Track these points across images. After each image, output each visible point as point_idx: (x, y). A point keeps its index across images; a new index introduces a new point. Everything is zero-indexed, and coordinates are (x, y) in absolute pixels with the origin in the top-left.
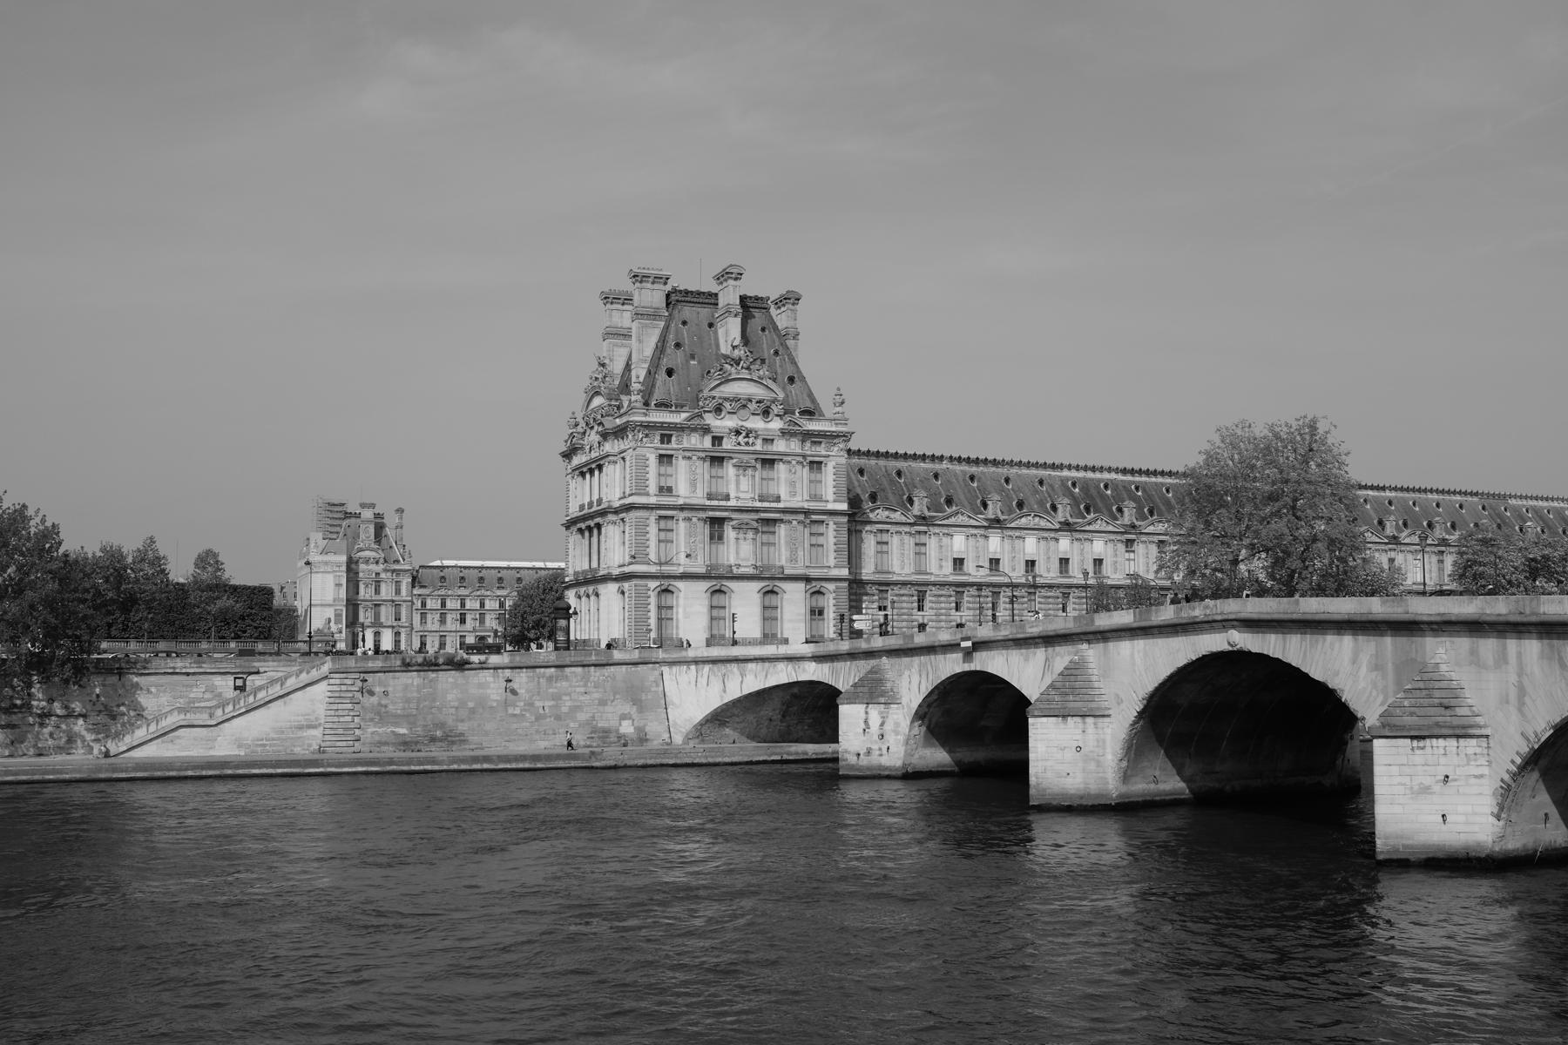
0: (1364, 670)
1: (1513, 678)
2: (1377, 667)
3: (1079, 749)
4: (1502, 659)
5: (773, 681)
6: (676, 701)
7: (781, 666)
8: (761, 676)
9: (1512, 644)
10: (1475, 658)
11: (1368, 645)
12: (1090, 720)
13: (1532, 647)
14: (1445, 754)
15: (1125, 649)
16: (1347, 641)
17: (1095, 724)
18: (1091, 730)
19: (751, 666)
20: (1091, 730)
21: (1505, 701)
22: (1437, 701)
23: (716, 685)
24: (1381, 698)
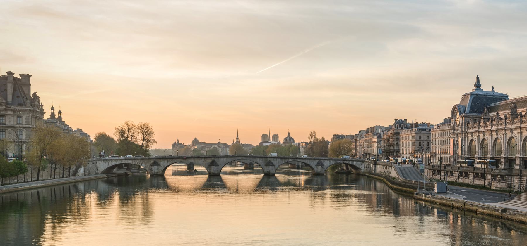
0: (261, 161)
1: (277, 161)
2: (263, 161)
4: (276, 160)
5: (117, 163)
6: (99, 166)
8: (115, 163)
9: (277, 159)
10: (274, 160)
11: (261, 159)
13: (279, 159)
15: (222, 159)
16: (259, 159)
21: (276, 163)
23: (107, 164)
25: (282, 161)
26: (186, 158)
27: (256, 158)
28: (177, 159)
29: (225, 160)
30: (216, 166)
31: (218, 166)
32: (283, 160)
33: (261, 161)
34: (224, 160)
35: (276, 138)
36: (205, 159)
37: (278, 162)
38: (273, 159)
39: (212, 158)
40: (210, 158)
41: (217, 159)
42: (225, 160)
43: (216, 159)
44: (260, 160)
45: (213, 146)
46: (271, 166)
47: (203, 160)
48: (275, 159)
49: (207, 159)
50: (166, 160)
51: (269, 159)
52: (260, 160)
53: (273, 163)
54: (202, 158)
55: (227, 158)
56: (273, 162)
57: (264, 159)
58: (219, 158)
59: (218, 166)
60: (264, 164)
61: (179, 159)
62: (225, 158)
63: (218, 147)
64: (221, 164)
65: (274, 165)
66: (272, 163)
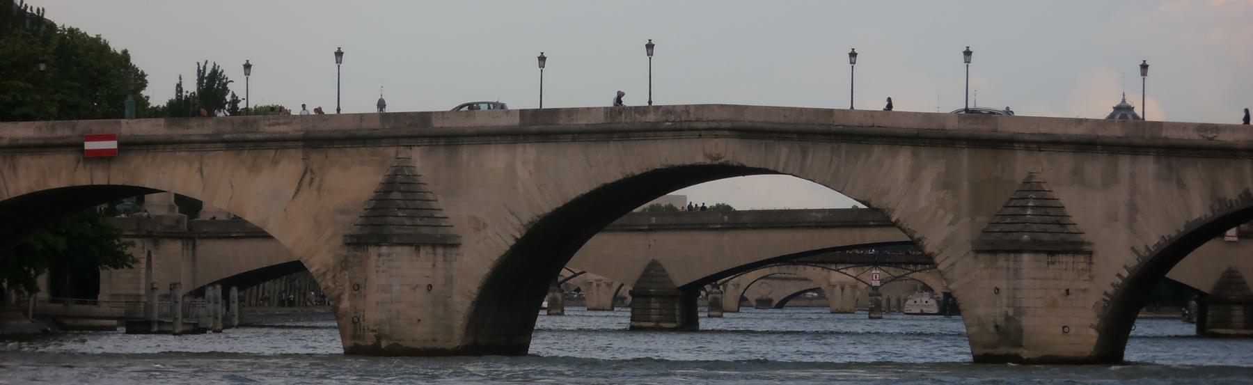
0: (927, 187)
2: (947, 183)
3: (430, 287)
4: (1111, 180)
9: (1125, 164)
11: (934, 166)
12: (440, 251)
13: (1148, 167)
14: (1066, 269)
15: (496, 158)
16: (903, 159)
17: (444, 255)
18: (440, 264)
20: (440, 264)
22: (1053, 219)
24: (950, 217)
25: (1181, 185)
26: (113, 145)
27: (878, 151)
28: (25, 161)
29: (523, 173)
30: (416, 243)
31: (448, 243)
32: (1194, 175)
36: (316, 158)
37: (1133, 209)
38: (1066, 161)
39: (391, 151)
46: (1036, 247)
48: (1095, 167)
49: (334, 154)
51: (1022, 165)
52: (914, 177)
54: (281, 143)
55: (550, 148)
58: (465, 153)
61: (45, 161)
62: (528, 153)
64: (479, 226)
65: (1077, 248)
66: (1061, 220)
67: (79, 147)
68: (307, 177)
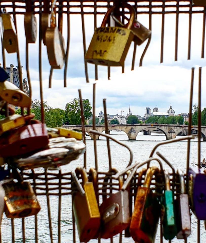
0: (165, 129)
1: (177, 129)
2: (166, 128)
4: (177, 128)
7: (72, 128)
9: (177, 127)
10: (174, 128)
11: (166, 127)
13: (179, 127)
15: (138, 127)
19: (69, 128)
29: (140, 128)
33: (165, 129)
34: (139, 128)
35: (149, 110)
36: (127, 127)
38: (174, 127)
40: (130, 126)
41: (135, 126)
42: (140, 128)
43: (134, 127)
44: (164, 128)
45: (115, 117)
47: (125, 127)
48: (176, 127)
50: (101, 127)
51: (171, 127)
52: (164, 128)
53: (174, 130)
54: (125, 126)
55: (142, 126)
56: (174, 129)
57: (167, 127)
58: (136, 126)
59: (135, 132)
60: (168, 131)
63: (118, 118)
64: (137, 131)
65: (175, 133)
67: (112, 126)
68: (126, 128)
